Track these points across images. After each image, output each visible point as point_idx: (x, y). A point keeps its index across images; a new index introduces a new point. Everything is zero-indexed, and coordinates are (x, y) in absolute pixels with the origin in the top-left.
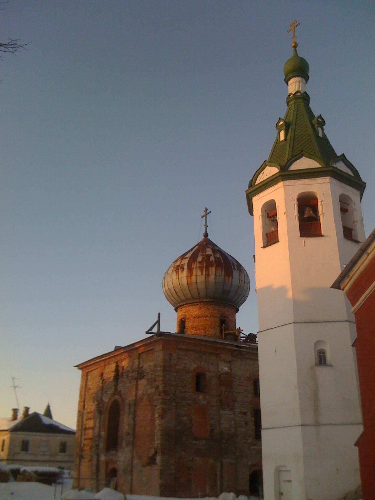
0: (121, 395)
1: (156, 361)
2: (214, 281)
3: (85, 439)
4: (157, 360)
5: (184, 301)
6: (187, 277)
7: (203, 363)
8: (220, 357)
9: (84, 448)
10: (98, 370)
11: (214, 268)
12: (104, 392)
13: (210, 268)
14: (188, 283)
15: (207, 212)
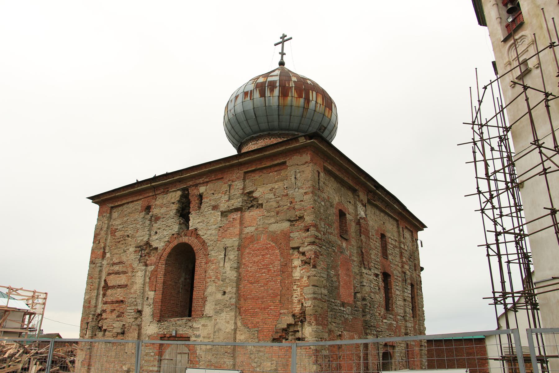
0: (198, 236)
1: (293, 179)
2: (314, 108)
3: (105, 303)
4: (295, 178)
5: (263, 131)
6: (279, 96)
7: (342, 198)
8: (358, 196)
9: (104, 316)
10: (140, 202)
11: (314, 93)
12: (153, 233)
13: (311, 92)
14: (279, 105)
15: (285, 38)
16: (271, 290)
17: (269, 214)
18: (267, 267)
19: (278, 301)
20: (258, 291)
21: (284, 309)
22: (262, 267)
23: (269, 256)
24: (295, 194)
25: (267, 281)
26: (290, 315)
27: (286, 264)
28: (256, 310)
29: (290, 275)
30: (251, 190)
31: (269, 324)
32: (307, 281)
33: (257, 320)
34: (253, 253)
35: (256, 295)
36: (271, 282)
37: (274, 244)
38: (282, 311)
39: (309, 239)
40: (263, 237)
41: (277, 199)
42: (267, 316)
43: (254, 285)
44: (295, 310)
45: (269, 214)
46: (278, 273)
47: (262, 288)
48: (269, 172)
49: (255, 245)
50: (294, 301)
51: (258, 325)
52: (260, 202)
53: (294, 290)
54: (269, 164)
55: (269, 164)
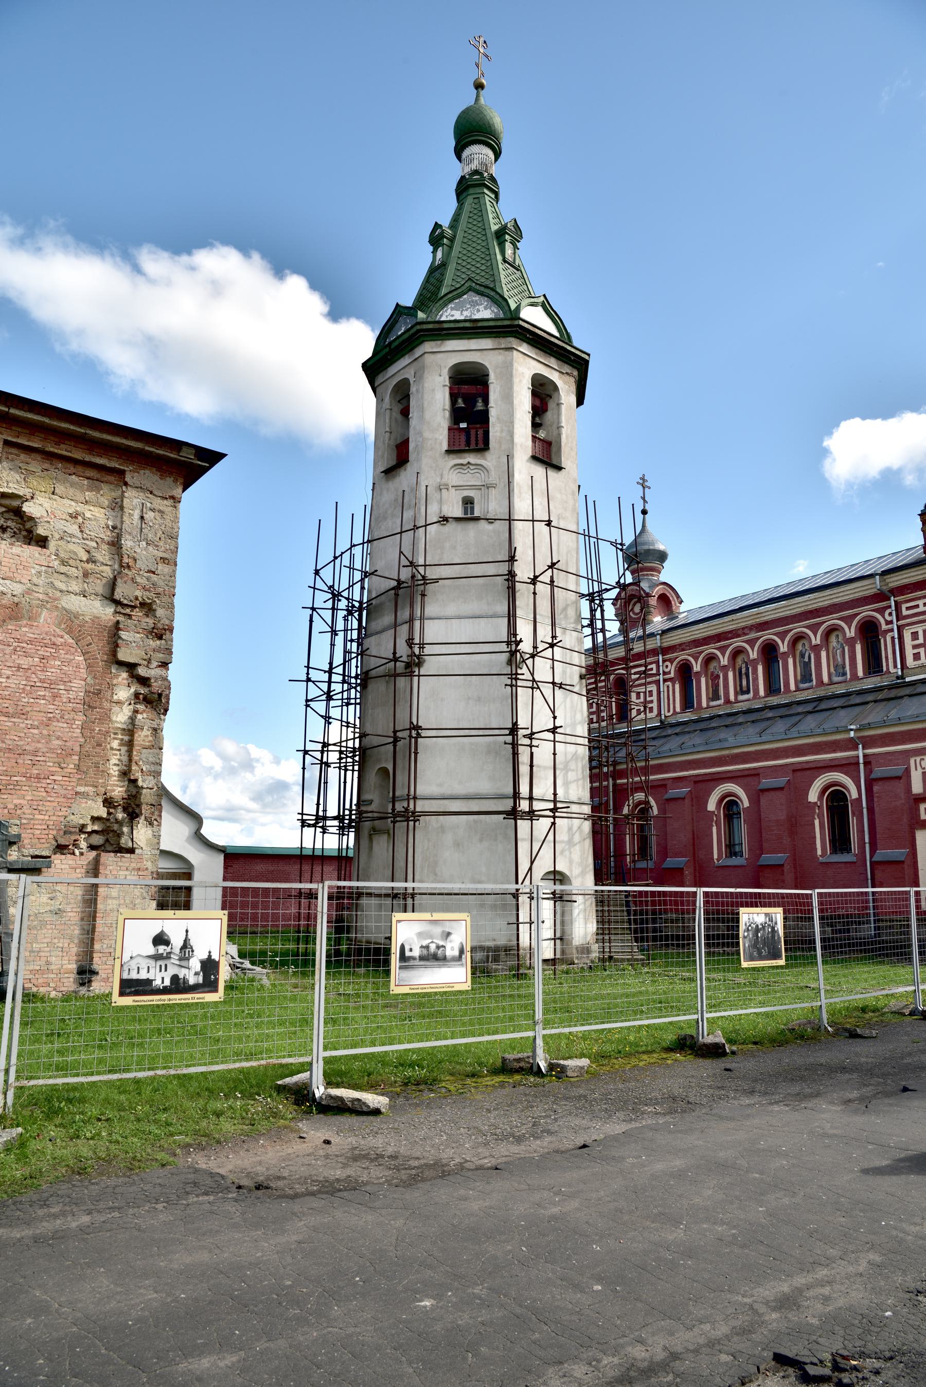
16: (58, 739)
17: (63, 569)
18: (52, 686)
19: (72, 766)
20: (23, 735)
21: (86, 785)
22: (38, 684)
23: (59, 663)
24: (138, 550)
25: (49, 719)
26: (100, 800)
27: (98, 693)
28: (15, 778)
29: (106, 717)
30: (16, 492)
31: (49, 813)
32: (151, 738)
33: (16, 801)
34: (16, 644)
35: (18, 743)
36: (58, 721)
37: (71, 641)
38: (81, 789)
39: (161, 655)
40: (45, 618)
41: (86, 542)
42: (44, 794)
43: (13, 720)
44: (114, 790)
45: (63, 569)
46: (78, 706)
47: (36, 731)
48: (70, 471)
49: (24, 629)
50: (112, 771)
51: (19, 812)
52: (41, 531)
53: (112, 749)
54: (78, 455)
55: (78, 455)
